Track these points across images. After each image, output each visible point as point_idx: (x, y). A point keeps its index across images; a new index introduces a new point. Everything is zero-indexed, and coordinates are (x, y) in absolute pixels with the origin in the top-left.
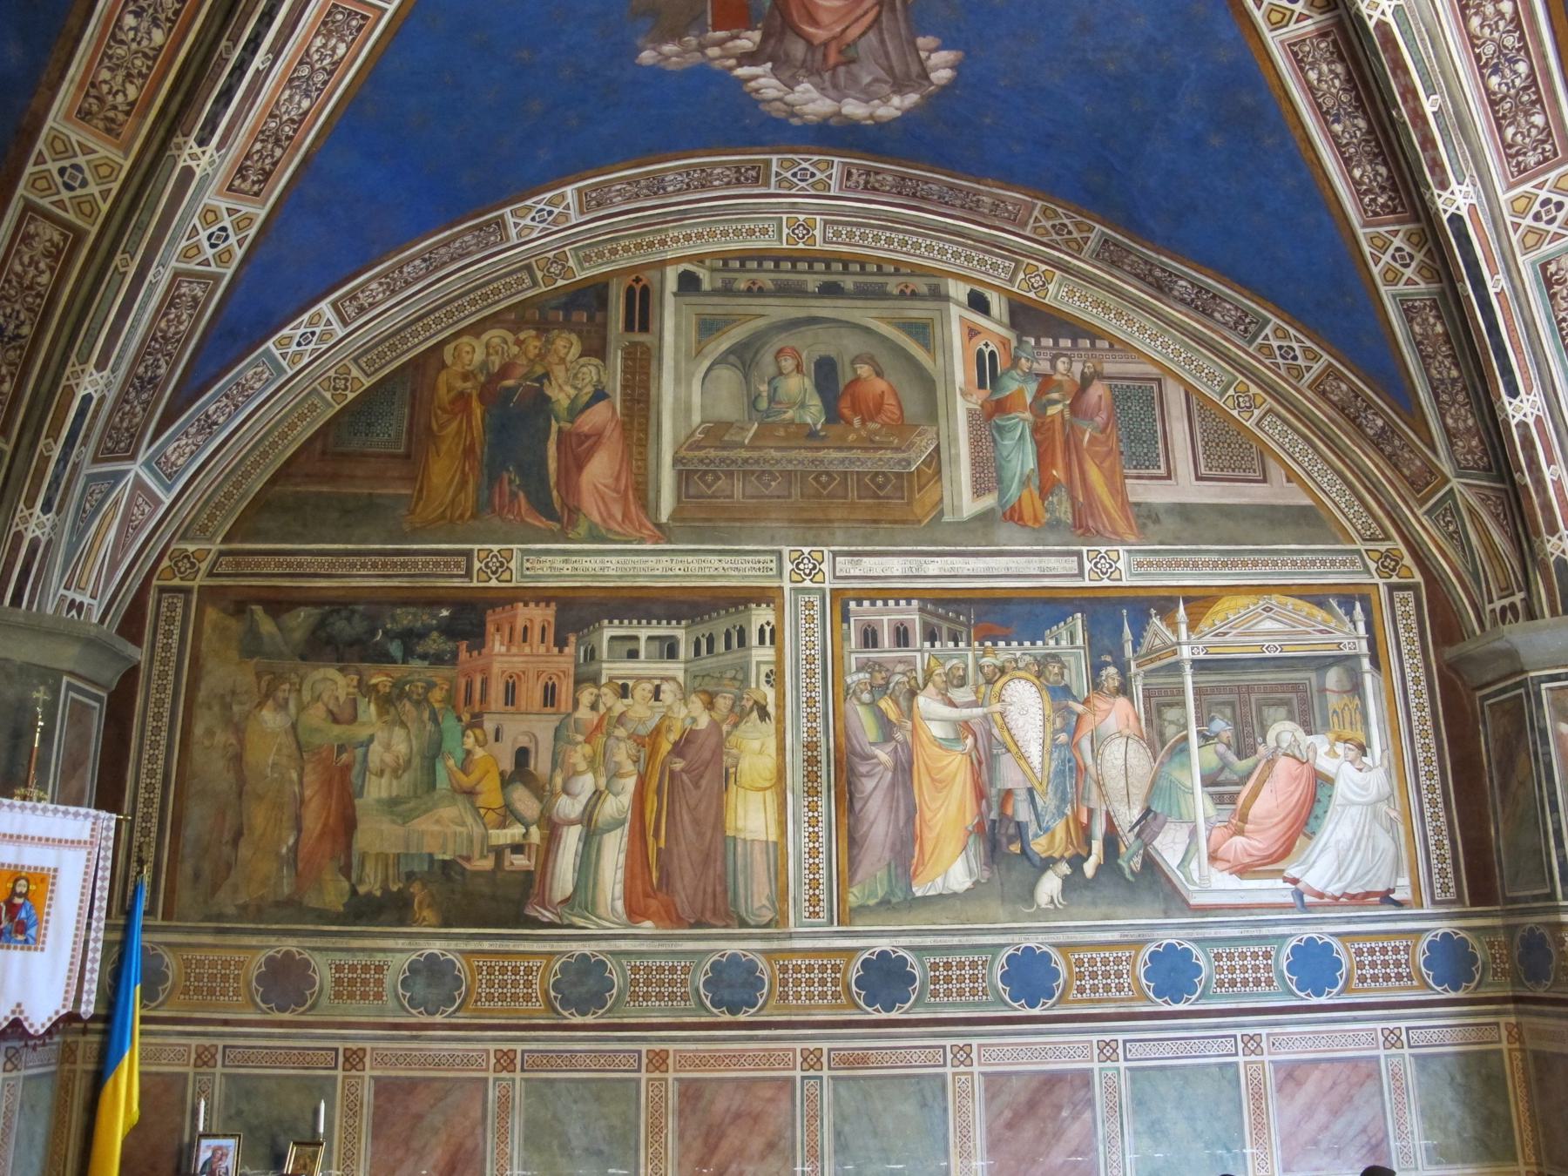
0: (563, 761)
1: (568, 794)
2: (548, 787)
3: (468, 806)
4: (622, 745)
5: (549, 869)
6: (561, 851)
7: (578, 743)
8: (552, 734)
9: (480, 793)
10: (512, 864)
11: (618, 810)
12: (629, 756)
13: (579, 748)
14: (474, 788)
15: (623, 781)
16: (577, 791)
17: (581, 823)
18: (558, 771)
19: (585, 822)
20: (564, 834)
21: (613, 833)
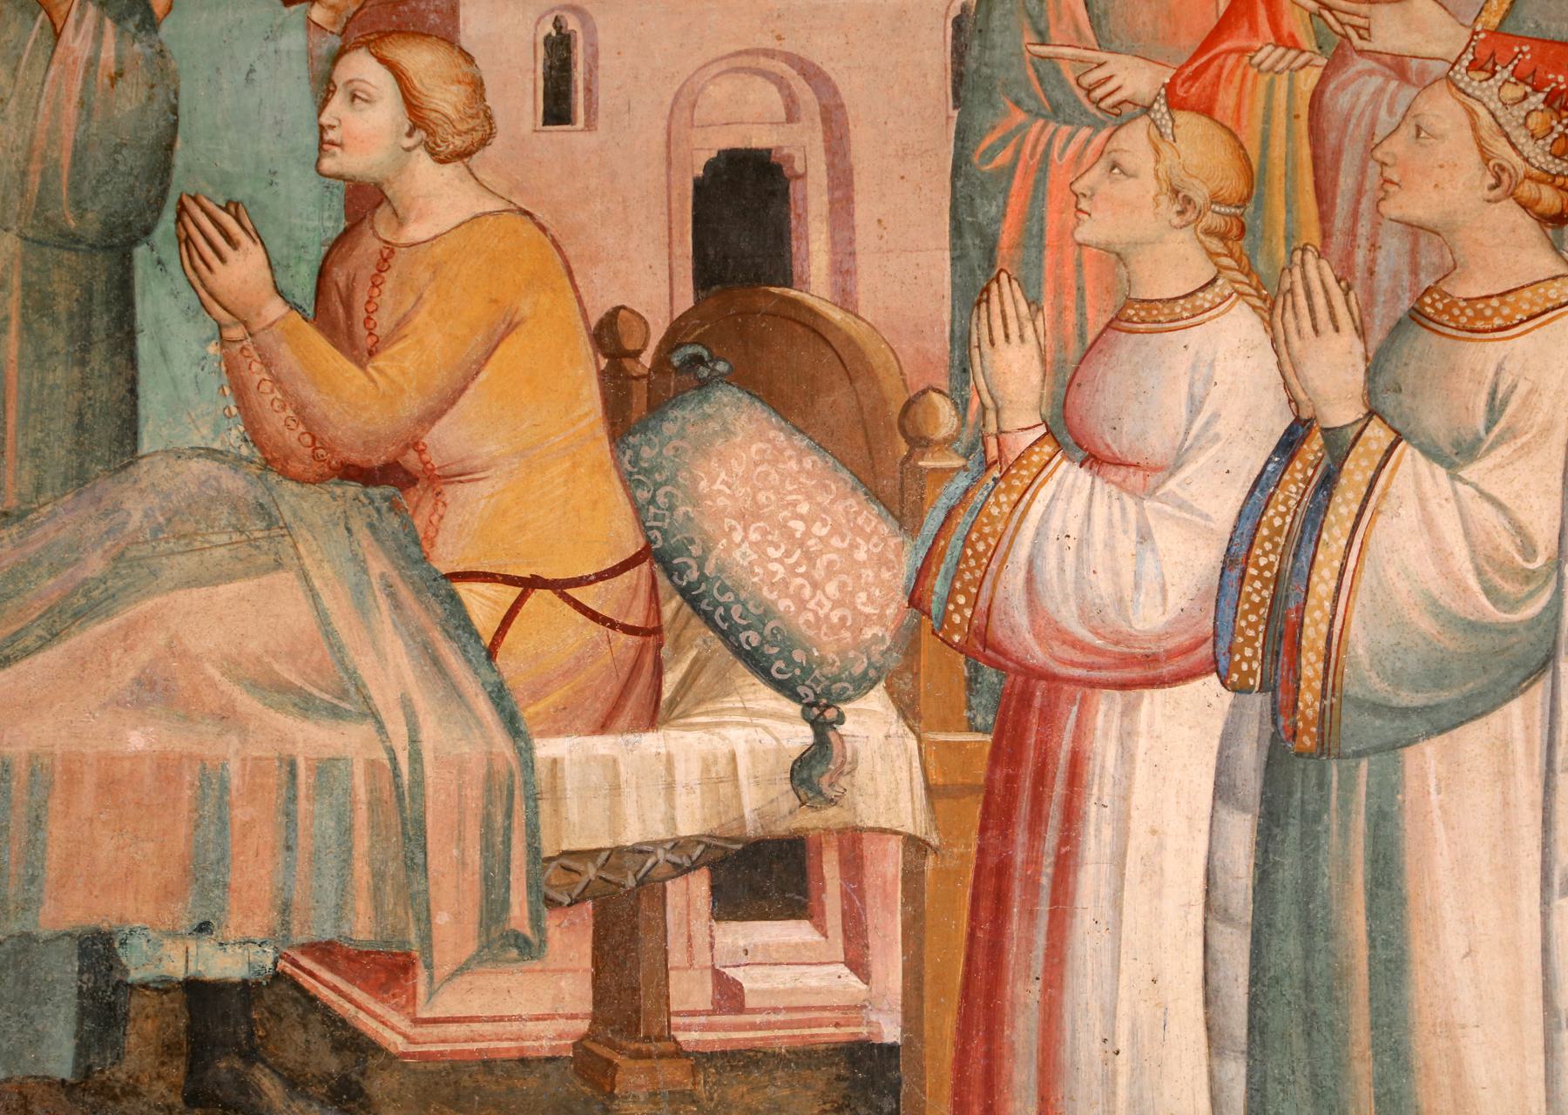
0: (1033, 236)
1: (1094, 460)
2: (944, 417)
3: (378, 565)
4: (1442, 110)
5: (1022, 1031)
6: (1091, 881)
7: (1121, 113)
8: (935, 55)
9: (462, 475)
10: (729, 995)
11: (1486, 563)
12: (1501, 182)
13: (1134, 141)
14: (415, 445)
15: (1483, 356)
16: (1157, 445)
17: (1213, 666)
18: (1008, 297)
19: (1250, 659)
20: (1104, 753)
21: (1474, 738)
